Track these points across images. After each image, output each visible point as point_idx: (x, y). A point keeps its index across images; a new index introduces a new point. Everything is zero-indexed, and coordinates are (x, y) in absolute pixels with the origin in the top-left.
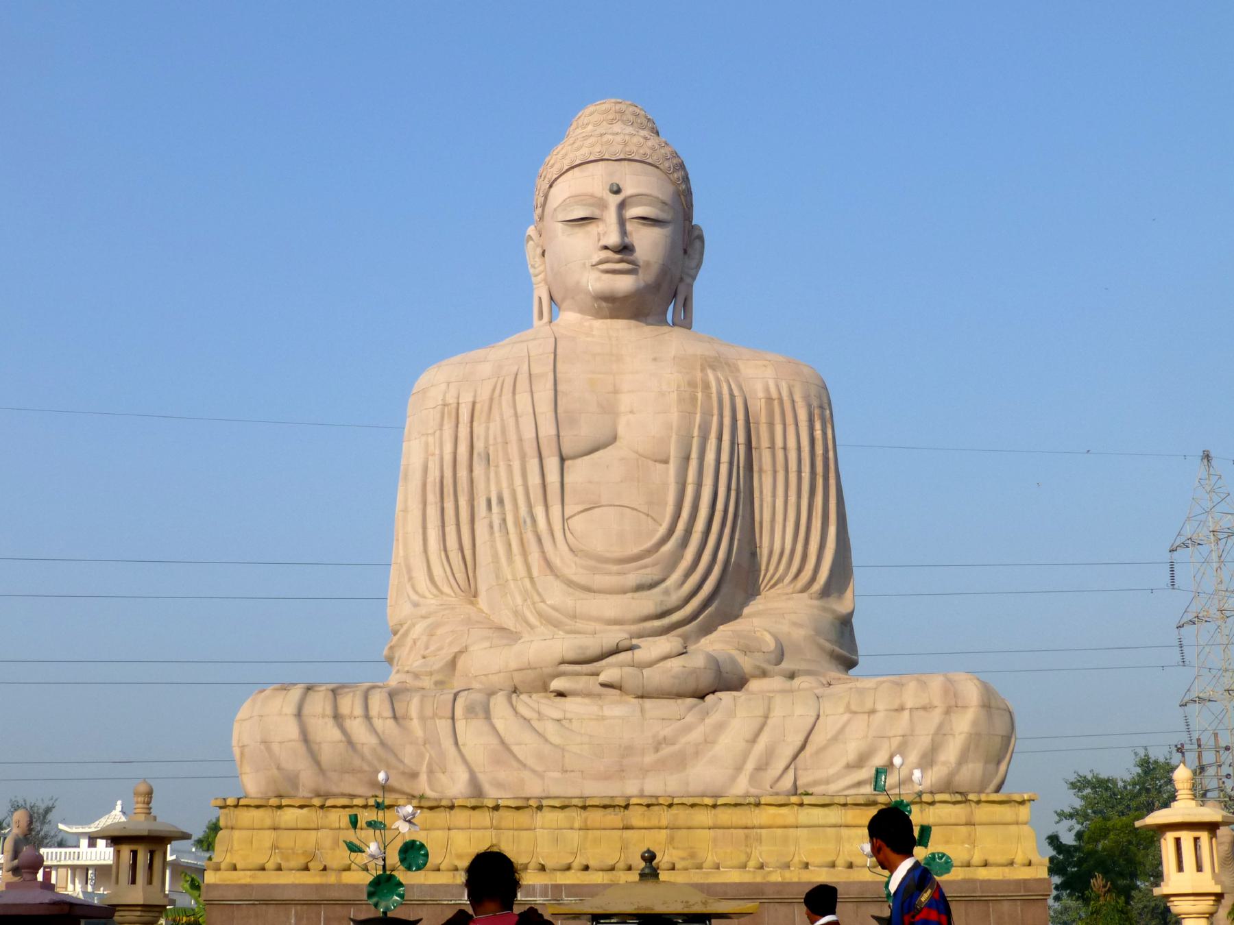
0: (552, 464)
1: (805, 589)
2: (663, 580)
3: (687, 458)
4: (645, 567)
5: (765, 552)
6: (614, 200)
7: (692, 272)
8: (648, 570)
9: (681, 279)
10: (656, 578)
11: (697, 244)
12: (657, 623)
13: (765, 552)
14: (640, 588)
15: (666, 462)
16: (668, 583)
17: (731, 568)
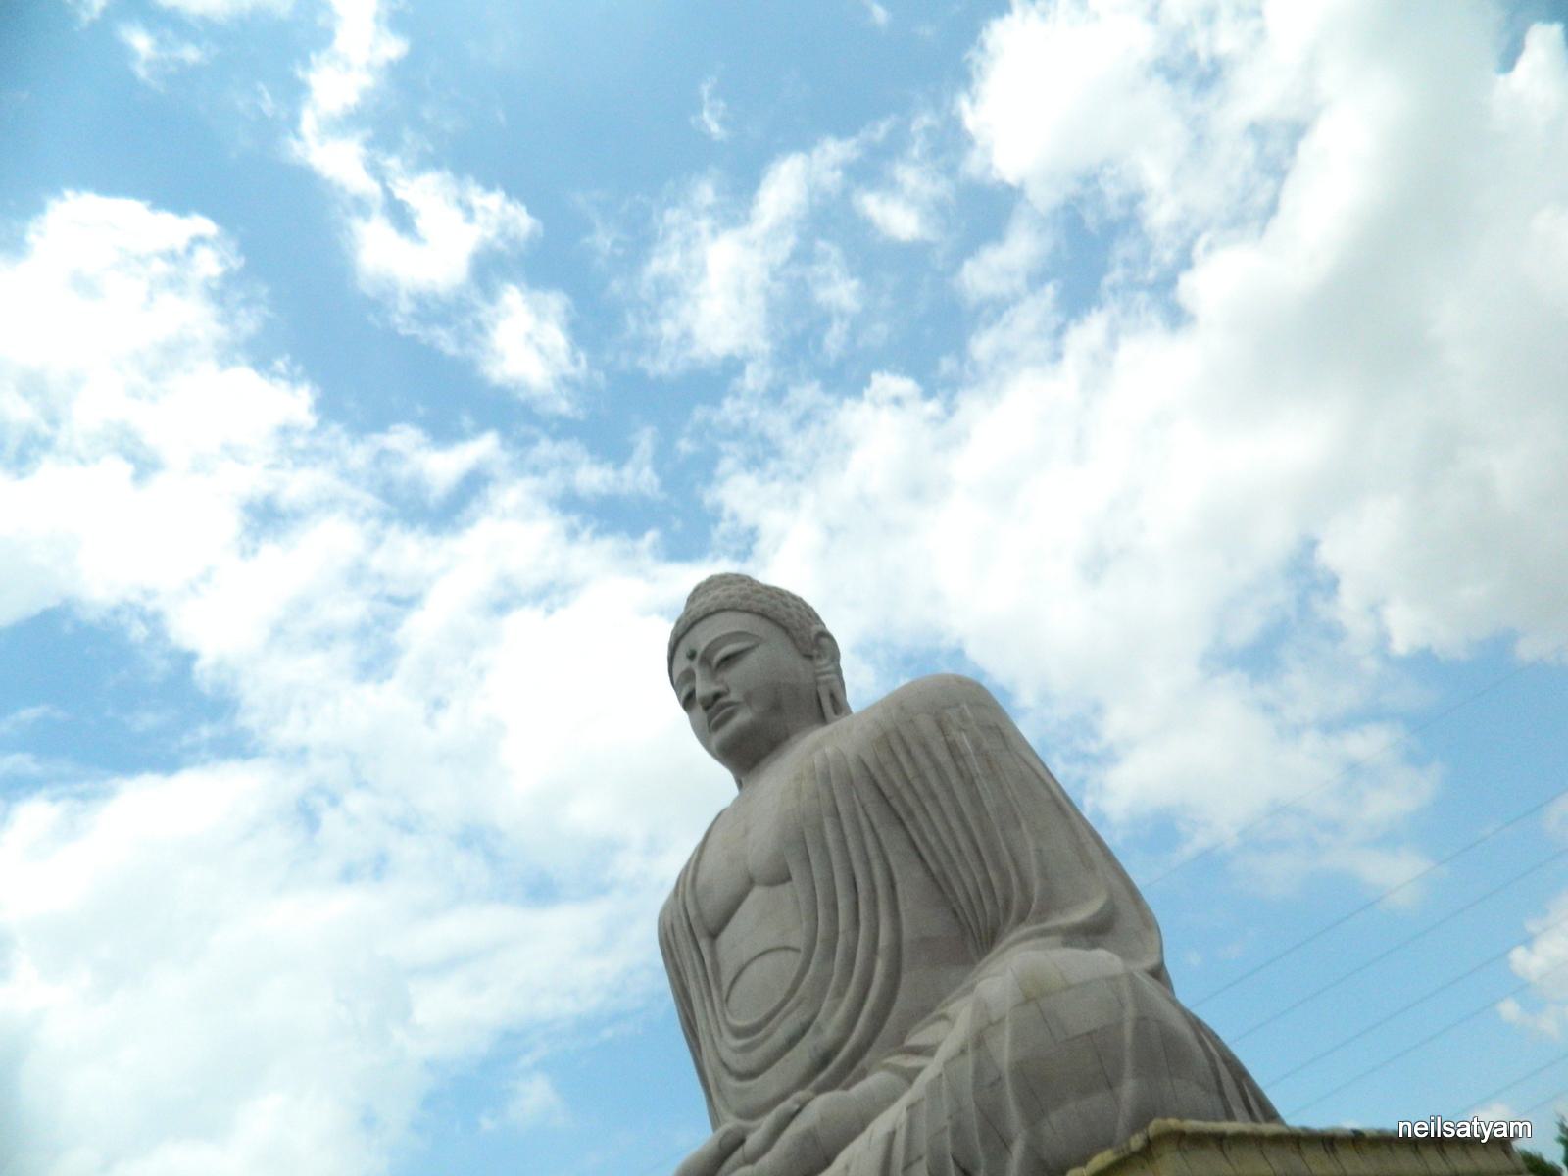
0: (703, 944)
1: (1022, 919)
2: (815, 1017)
3: (807, 858)
4: (789, 1013)
5: (963, 901)
6: (695, 663)
7: (831, 668)
8: (794, 1015)
9: (817, 683)
10: (805, 1018)
11: (824, 641)
12: (822, 1076)
13: (963, 901)
14: (792, 1041)
15: (789, 878)
16: (819, 1019)
17: (905, 949)
